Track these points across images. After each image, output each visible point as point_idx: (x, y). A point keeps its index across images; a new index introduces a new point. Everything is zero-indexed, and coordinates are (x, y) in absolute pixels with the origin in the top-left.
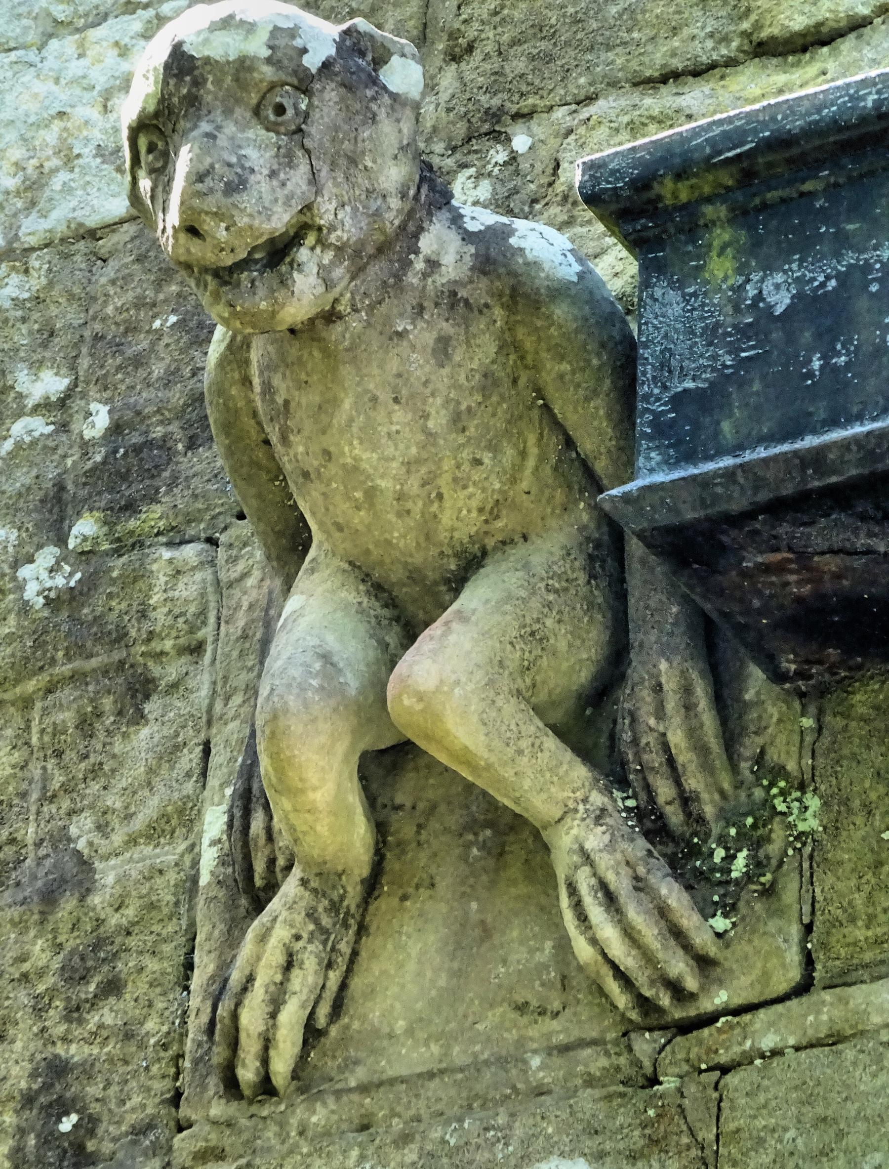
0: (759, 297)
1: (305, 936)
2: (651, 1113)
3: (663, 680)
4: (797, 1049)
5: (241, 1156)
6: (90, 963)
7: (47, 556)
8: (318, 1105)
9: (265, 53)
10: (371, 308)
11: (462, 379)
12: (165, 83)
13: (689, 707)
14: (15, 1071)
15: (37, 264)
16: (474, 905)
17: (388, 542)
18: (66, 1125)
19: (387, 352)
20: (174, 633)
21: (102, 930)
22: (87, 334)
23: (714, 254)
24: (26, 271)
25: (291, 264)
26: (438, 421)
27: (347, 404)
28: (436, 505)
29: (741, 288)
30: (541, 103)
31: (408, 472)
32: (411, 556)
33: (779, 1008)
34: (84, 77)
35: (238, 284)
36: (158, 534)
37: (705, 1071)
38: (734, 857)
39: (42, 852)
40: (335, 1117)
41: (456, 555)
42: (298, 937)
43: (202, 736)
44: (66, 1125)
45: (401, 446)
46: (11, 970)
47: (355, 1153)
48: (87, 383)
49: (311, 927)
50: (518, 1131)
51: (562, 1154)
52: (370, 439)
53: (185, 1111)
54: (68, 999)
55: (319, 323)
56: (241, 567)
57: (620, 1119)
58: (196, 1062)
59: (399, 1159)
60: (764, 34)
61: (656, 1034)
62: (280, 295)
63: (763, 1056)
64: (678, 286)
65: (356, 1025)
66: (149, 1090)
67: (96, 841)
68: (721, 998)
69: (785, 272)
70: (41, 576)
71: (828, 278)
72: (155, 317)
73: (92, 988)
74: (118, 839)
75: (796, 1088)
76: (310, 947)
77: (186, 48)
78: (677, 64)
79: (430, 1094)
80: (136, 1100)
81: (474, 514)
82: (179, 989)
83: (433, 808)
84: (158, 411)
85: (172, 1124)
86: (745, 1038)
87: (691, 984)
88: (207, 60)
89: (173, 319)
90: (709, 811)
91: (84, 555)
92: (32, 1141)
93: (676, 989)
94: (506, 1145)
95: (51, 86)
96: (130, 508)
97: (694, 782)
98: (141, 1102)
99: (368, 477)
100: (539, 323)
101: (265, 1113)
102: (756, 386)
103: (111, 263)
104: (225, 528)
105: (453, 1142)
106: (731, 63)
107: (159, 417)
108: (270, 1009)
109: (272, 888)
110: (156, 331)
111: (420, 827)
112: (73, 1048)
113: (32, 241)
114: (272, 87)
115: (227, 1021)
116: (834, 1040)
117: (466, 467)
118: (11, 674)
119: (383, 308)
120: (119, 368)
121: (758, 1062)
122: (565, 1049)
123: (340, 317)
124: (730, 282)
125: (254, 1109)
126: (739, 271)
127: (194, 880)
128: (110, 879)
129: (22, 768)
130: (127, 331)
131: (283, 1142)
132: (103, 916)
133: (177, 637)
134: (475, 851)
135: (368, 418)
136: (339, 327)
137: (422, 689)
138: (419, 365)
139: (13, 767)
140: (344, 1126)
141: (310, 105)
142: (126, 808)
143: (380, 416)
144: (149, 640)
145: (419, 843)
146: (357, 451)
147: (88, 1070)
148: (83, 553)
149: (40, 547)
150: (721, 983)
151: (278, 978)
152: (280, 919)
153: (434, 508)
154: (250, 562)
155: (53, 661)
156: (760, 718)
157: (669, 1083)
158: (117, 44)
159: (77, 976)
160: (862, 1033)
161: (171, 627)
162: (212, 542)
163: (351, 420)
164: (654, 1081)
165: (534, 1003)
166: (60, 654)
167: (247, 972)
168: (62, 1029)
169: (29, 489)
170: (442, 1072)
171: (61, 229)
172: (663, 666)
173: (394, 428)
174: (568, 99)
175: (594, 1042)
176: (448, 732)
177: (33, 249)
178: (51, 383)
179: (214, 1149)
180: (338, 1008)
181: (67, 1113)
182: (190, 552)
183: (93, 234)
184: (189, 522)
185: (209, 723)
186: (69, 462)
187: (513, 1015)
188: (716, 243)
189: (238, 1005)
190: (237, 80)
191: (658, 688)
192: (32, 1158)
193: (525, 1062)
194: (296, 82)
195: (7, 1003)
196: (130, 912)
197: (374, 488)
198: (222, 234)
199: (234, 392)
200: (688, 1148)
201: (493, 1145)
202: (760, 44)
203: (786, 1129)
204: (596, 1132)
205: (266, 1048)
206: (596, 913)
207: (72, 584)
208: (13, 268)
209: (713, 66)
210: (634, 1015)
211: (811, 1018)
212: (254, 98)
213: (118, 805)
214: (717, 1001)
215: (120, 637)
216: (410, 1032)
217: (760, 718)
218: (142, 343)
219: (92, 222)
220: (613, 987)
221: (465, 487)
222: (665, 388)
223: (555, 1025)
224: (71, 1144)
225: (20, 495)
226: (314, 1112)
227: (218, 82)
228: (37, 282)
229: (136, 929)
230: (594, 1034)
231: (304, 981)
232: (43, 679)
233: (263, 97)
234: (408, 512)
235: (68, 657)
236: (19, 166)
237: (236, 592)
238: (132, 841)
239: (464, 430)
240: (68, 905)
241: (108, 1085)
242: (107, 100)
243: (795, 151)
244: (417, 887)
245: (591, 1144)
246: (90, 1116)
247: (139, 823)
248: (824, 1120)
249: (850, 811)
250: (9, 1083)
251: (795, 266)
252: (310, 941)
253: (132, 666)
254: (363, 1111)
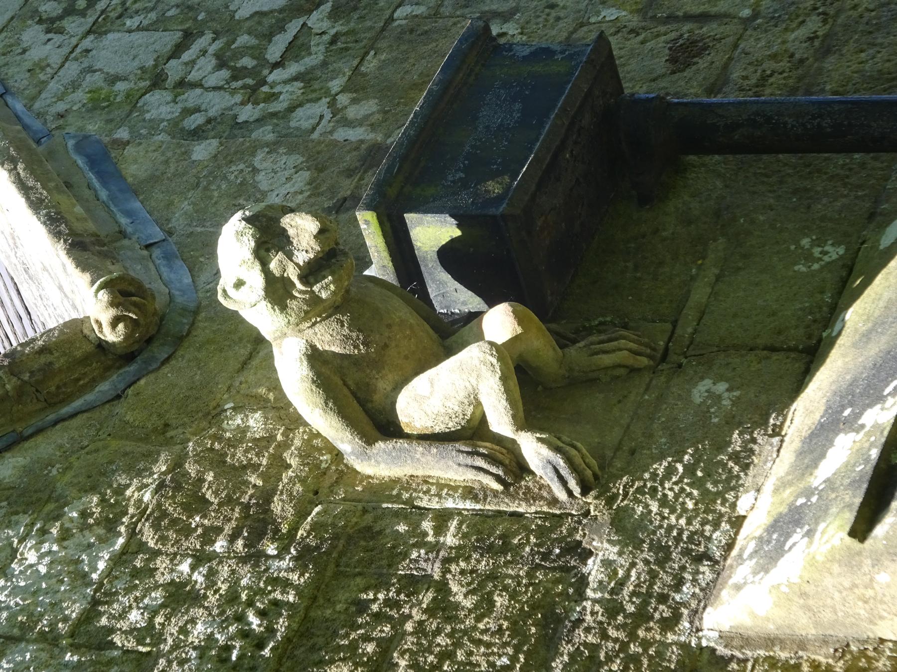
68: (662, 343)
91: (283, 551)
122: (647, 389)
157: (684, 361)
160: (706, 306)
175: (651, 380)
205: (584, 462)
210: (652, 363)
230: (648, 380)
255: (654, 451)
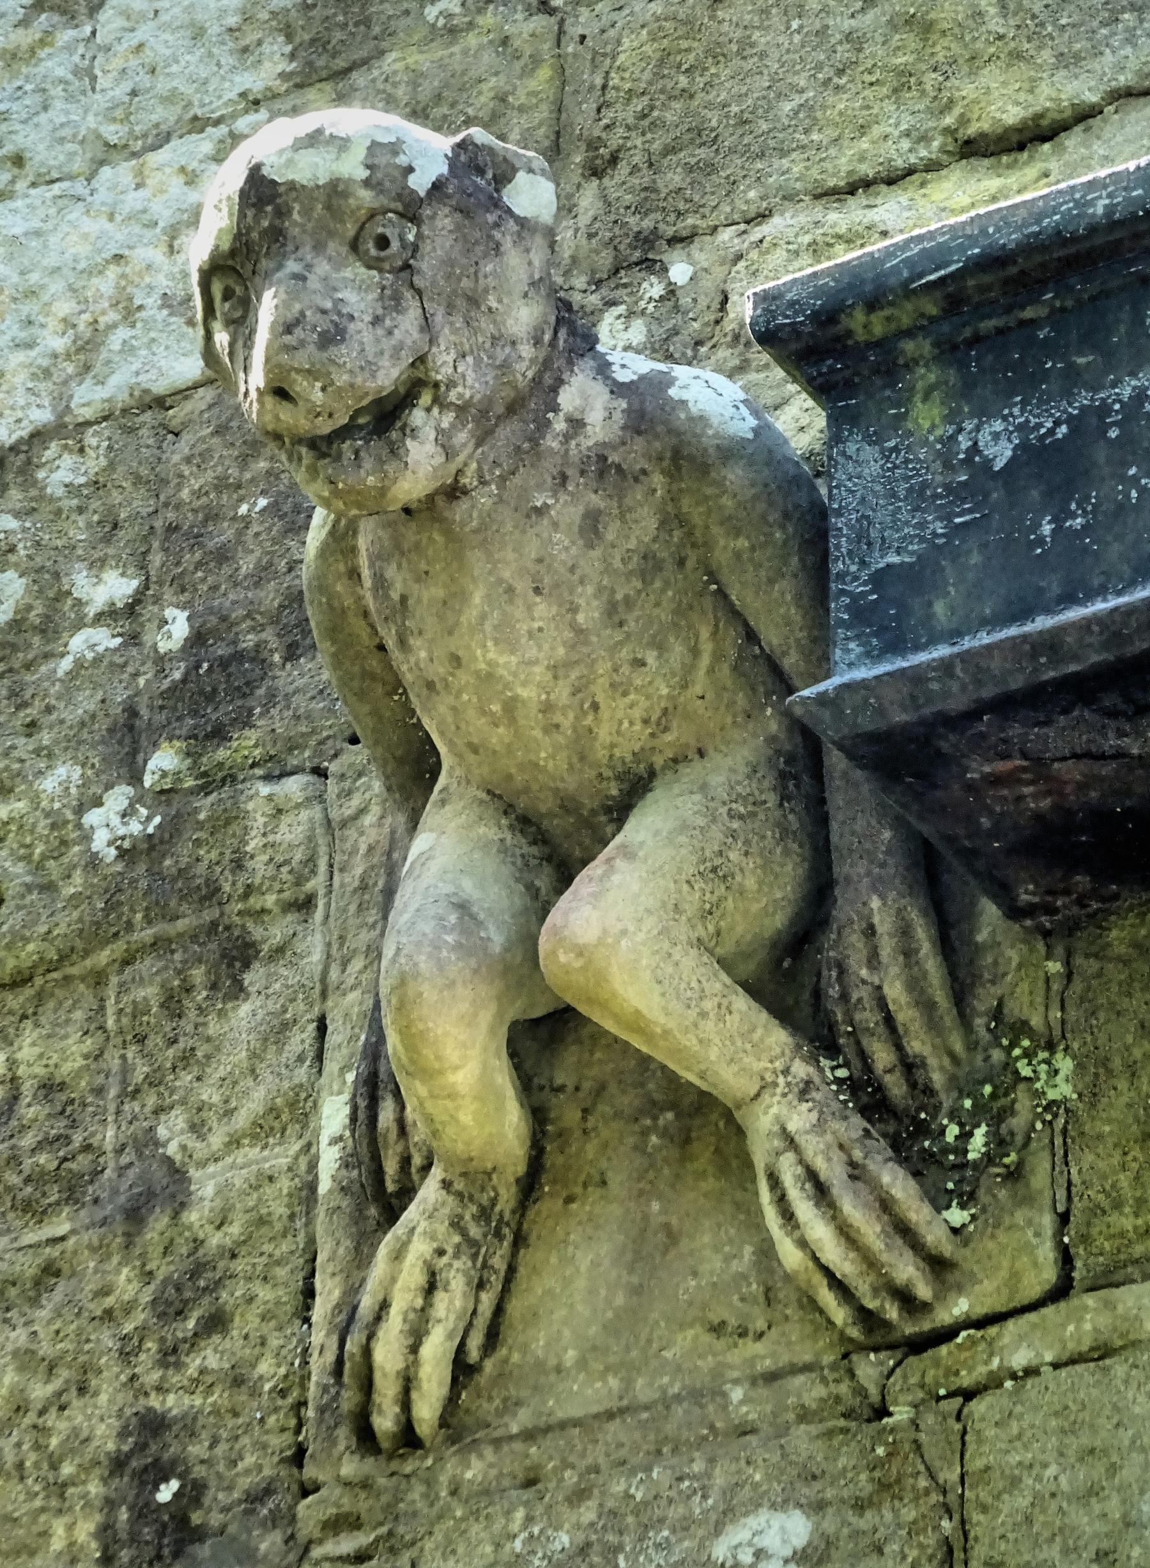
0: (975, 449)
1: (450, 1251)
2: (880, 1451)
3: (876, 920)
4: (1056, 1366)
5: (381, 1524)
6: (188, 1294)
7: (118, 797)
8: (473, 1458)
9: (364, 174)
10: (503, 479)
11: (617, 563)
12: (242, 215)
13: (908, 953)
14: (101, 1429)
15: (94, 442)
16: (655, 1206)
17: (536, 765)
18: (166, 1493)
19: (524, 532)
20: (277, 886)
21: (201, 1252)
22: (158, 524)
23: (918, 398)
24: (82, 450)
25: (403, 429)
26: (589, 614)
27: (477, 598)
28: (590, 717)
29: (953, 438)
30: (702, 224)
31: (556, 677)
32: (563, 780)
33: (1032, 1317)
34: (145, 211)
35: (339, 457)
36: (252, 766)
37: (945, 1397)
38: (970, 1134)
39: (125, 1160)
40: (493, 1472)
41: (619, 778)
42: (441, 1252)
43: (316, 1011)
44: (166, 1493)
45: (546, 647)
46: (91, 1306)
47: (520, 1514)
48: (161, 583)
49: (457, 1239)
50: (719, 1480)
51: (773, 1506)
52: (507, 639)
53: (310, 1472)
54: (162, 1340)
55: (440, 501)
56: (356, 802)
57: (842, 1462)
58: (321, 1410)
59: (574, 1519)
60: (972, 130)
61: (882, 1355)
62: (390, 468)
63: (1014, 1376)
64: (876, 440)
65: (516, 1357)
66: (264, 1447)
67: (190, 1144)
68: (961, 1307)
69: (1005, 418)
70: (111, 822)
71: (1057, 423)
72: (241, 500)
73: (191, 1324)
74: (217, 1140)
75: (1056, 1414)
76: (457, 1264)
77: (265, 171)
78: (867, 170)
79: (609, 1438)
80: (249, 1460)
81: (638, 727)
82: (298, 1322)
83: (601, 1089)
84: (249, 616)
85: (295, 1487)
86: (991, 1355)
87: (923, 1291)
88: (292, 186)
89: (262, 502)
90: (938, 1079)
91: (164, 795)
92: (123, 1515)
93: (905, 1298)
94: (705, 1497)
95: (103, 223)
96: (219, 734)
97: (916, 1046)
98: (256, 1462)
99: (507, 686)
100: (709, 491)
101: (408, 1469)
102: (975, 559)
103: (185, 437)
104: (336, 756)
105: (639, 1496)
106: (932, 167)
107: (249, 623)
108: (410, 1341)
109: (407, 1193)
110: (243, 517)
111: (585, 1111)
112: (171, 1399)
113: (87, 413)
114: (372, 215)
115: (358, 1358)
116: (1101, 1352)
117: (626, 669)
118: (79, 944)
119: (517, 480)
120: (199, 565)
121: (1009, 1384)
122: (772, 1377)
123: (465, 492)
124: (939, 432)
125: (394, 1465)
126: (949, 419)
127: (312, 1187)
128: (209, 1190)
129: (96, 1058)
130: (206, 520)
131: (432, 1505)
132: (201, 1235)
133: (281, 891)
134: (654, 1139)
135: (504, 613)
136: (464, 505)
137: (581, 941)
138: (563, 544)
139: (86, 1057)
140: (506, 1483)
141: (419, 236)
142: (226, 1102)
143: (519, 612)
144: (246, 896)
145: (585, 1132)
146: (491, 655)
147: (189, 1426)
148: (162, 792)
149: (109, 787)
150: (960, 1289)
151: (419, 1302)
152: (419, 1230)
153: (589, 720)
154: (367, 796)
155: (129, 926)
156: (996, 963)
157: (901, 1414)
158: (182, 169)
159: (171, 1311)
160: (1135, 1344)
161: (273, 878)
162: (320, 773)
163: (483, 617)
164: (882, 1412)
165: (733, 1322)
166: (139, 916)
167: (381, 1297)
168: (156, 1375)
169: (93, 716)
170: (622, 1411)
171: (122, 399)
172: (875, 903)
173: (536, 625)
174: (736, 217)
175: (807, 1368)
176: (614, 995)
177: (88, 424)
178: (116, 587)
179: (348, 1515)
180: (493, 1337)
181: (166, 1480)
182: (294, 787)
183: (160, 403)
184: (291, 750)
185: (324, 995)
186: (142, 681)
187: (707, 1338)
188: (920, 385)
189: (371, 1337)
190: (328, 207)
191: (870, 931)
192: (124, 1536)
193: (724, 1395)
194: (400, 208)
195: (87, 1347)
196: (235, 1230)
197: (515, 699)
198: (318, 396)
199: (339, 588)
200: (927, 1492)
201: (689, 1497)
202: (968, 142)
203: (1045, 1466)
204: (814, 1477)
206: (804, 1209)
207: (150, 830)
208: (66, 447)
209: (910, 172)
210: (854, 1333)
211: (1071, 1328)
212: (351, 229)
213: (216, 1099)
214: (956, 1312)
215: (211, 894)
216: (582, 1363)
217: (996, 963)
218: (225, 533)
219: (160, 387)
220: (827, 1298)
221: (625, 694)
222: (863, 563)
223: (759, 1348)
224: (172, 1517)
225: (83, 724)
226: (468, 1467)
227: (306, 212)
228: (94, 463)
229: (243, 1250)
230: (808, 1358)
231: (450, 1304)
232: (117, 949)
233: (362, 228)
234: (557, 726)
235: (149, 921)
236: (68, 323)
237: (351, 833)
238: (234, 1142)
239: (621, 624)
240: (158, 1224)
241: (215, 1442)
242: (173, 238)
243: (1013, 270)
244: (585, 1185)
245: (808, 1492)
246: (195, 1481)
247: (242, 1120)
248: (1092, 1451)
249: (1110, 1072)
250: (96, 1443)
251: (1016, 411)
252: (456, 1255)
253: (227, 928)
254: (528, 1462)
255: (518, 1545)
